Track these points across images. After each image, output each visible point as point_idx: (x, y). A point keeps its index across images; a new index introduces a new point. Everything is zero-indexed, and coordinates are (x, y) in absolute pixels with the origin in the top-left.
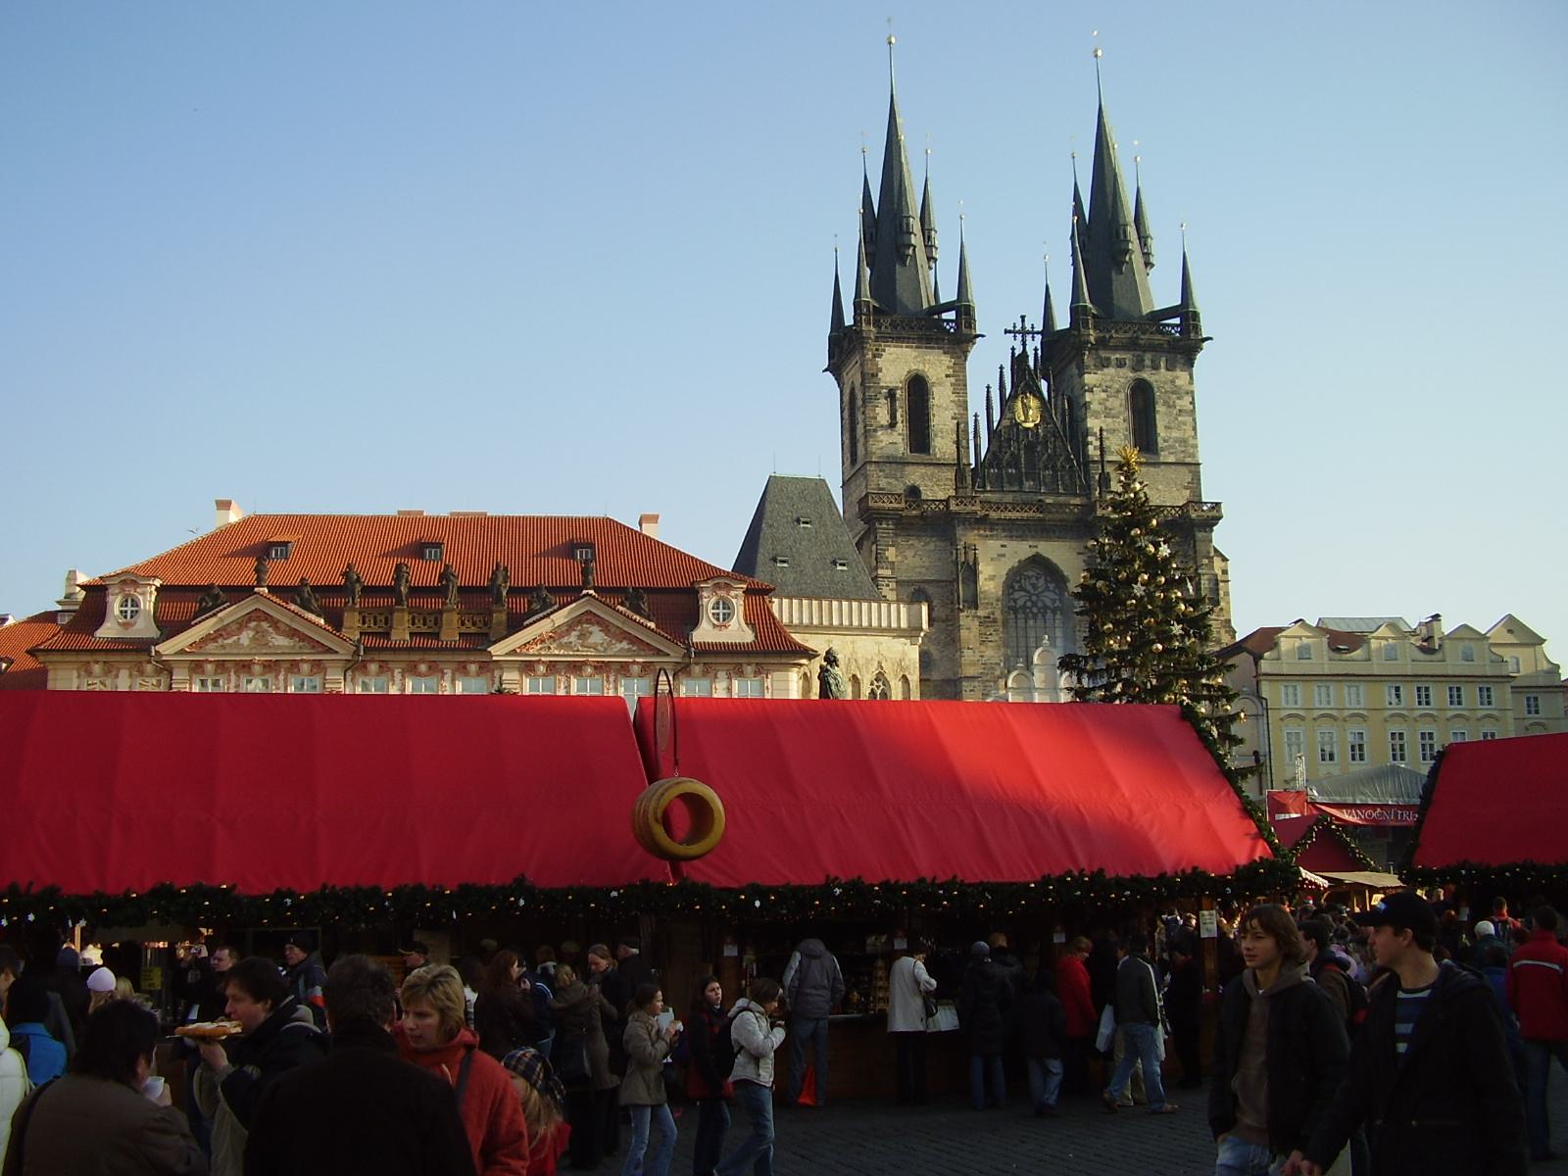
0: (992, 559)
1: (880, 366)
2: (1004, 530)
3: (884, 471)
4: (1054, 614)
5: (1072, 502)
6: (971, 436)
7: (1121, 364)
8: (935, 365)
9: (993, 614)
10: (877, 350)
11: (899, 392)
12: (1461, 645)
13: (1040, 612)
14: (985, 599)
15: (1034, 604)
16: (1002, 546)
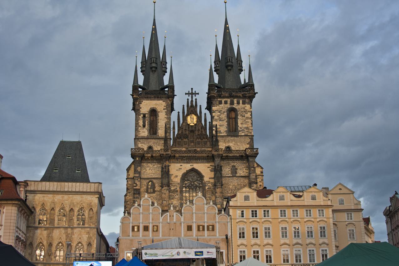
0: (177, 170)
1: (141, 107)
2: (182, 160)
3: (140, 141)
4: (199, 188)
5: (207, 150)
6: (172, 129)
7: (226, 103)
8: (160, 105)
9: (177, 189)
10: (140, 101)
11: (147, 115)
12: (311, 194)
13: (194, 188)
14: (174, 184)
15: (192, 185)
16: (181, 166)
